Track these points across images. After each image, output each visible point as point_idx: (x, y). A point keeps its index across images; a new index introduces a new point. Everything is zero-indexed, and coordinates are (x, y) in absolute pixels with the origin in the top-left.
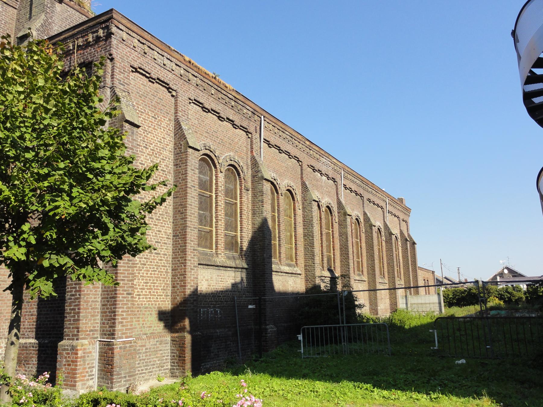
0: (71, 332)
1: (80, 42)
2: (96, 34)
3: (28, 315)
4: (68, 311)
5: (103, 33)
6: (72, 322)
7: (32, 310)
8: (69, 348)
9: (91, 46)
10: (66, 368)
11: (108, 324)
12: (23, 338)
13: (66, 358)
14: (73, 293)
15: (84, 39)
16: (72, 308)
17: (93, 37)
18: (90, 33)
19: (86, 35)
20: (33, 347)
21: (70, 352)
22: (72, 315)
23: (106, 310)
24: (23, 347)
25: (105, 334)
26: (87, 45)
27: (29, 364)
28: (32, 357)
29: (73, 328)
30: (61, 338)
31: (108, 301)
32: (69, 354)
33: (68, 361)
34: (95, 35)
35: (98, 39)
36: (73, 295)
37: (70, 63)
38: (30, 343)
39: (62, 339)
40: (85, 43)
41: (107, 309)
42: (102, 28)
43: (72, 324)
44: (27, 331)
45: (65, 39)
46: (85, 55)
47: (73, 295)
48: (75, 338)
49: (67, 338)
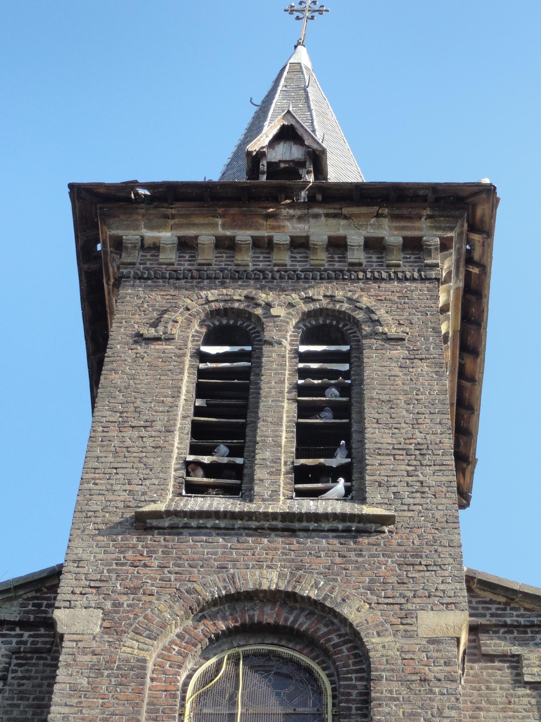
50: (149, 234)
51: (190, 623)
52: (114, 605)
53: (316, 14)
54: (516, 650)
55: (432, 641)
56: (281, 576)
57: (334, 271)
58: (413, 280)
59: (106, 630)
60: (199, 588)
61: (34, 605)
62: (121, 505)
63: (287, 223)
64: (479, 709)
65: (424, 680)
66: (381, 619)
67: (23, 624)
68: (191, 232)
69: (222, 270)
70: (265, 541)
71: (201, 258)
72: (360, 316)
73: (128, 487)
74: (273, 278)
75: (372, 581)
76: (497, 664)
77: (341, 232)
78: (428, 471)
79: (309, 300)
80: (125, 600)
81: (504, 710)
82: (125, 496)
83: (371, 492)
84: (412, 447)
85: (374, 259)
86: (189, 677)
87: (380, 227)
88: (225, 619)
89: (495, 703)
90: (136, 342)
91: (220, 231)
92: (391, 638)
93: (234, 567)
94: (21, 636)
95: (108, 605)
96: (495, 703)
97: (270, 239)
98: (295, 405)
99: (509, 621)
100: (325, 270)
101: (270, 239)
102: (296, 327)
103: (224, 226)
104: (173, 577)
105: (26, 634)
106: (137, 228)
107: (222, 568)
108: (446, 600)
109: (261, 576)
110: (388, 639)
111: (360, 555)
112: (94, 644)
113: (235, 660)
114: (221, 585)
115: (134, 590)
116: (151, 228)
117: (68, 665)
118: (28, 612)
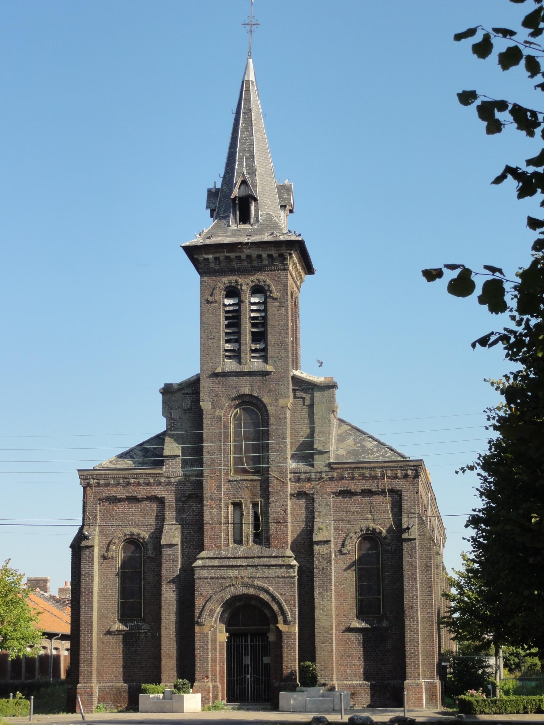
0: (413, 675)
1: (389, 473)
2: (405, 472)
3: (350, 665)
4: (409, 662)
5: (412, 473)
6: (413, 669)
7: (354, 662)
8: (415, 685)
9: (399, 479)
10: (413, 697)
11: (428, 671)
12: (346, 681)
13: (412, 690)
14: (412, 652)
15: (393, 472)
16: (412, 660)
17: (401, 473)
18: (399, 469)
19: (394, 470)
20: (360, 686)
21: (416, 687)
22: (413, 665)
23: (426, 662)
24: (349, 686)
25: (426, 678)
26: (396, 477)
27: (358, 697)
28: (361, 693)
29: (414, 673)
30: (404, 678)
31: (428, 657)
32: (415, 688)
33: (415, 692)
34: (404, 472)
35: (406, 476)
36: (412, 653)
37: (378, 486)
38: (358, 684)
39: (405, 679)
40: (394, 475)
41: (428, 662)
42: (412, 470)
43: (413, 671)
44: (350, 676)
45: (374, 468)
46: (393, 484)
47: (412, 653)
48: (417, 679)
49: (409, 679)
50: (206, 257)
51: (230, 402)
52: (213, 400)
53: (254, 27)
54: (304, 395)
55: (282, 408)
56: (249, 389)
57: (259, 267)
58: (281, 270)
59: (212, 408)
60: (231, 394)
61: (195, 388)
62: (211, 368)
63: (245, 250)
64: (295, 413)
65: (280, 419)
66: (271, 401)
67: (193, 393)
68: (218, 255)
69: (228, 268)
70: (245, 378)
71: (221, 265)
72: (266, 288)
73: (211, 361)
74: (242, 271)
75: (269, 390)
76: (300, 399)
77: (260, 253)
78: (283, 351)
79: (252, 281)
80: (215, 399)
81: (300, 412)
82: (211, 364)
83: (270, 361)
84: (279, 343)
85: (270, 261)
86: (231, 415)
87: (270, 250)
88: (237, 400)
89: (298, 411)
90: (207, 303)
91: (226, 254)
92: (273, 407)
93: (238, 387)
94: (193, 396)
95: (212, 401)
96: (298, 411)
97: (240, 257)
98: (251, 324)
99: (302, 387)
100: (257, 267)
101: (240, 257)
102: (250, 290)
103: (228, 252)
104: (225, 391)
105: (194, 396)
106: (202, 254)
107: (236, 387)
108: (285, 395)
109: (245, 390)
110: (272, 407)
111: (266, 382)
112: (210, 412)
113: (241, 409)
114: (236, 393)
115: (217, 396)
116: (206, 254)
117: (205, 418)
118: (193, 390)
